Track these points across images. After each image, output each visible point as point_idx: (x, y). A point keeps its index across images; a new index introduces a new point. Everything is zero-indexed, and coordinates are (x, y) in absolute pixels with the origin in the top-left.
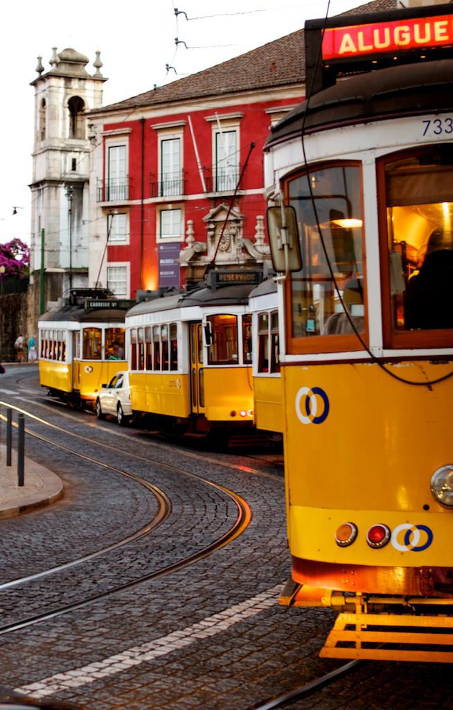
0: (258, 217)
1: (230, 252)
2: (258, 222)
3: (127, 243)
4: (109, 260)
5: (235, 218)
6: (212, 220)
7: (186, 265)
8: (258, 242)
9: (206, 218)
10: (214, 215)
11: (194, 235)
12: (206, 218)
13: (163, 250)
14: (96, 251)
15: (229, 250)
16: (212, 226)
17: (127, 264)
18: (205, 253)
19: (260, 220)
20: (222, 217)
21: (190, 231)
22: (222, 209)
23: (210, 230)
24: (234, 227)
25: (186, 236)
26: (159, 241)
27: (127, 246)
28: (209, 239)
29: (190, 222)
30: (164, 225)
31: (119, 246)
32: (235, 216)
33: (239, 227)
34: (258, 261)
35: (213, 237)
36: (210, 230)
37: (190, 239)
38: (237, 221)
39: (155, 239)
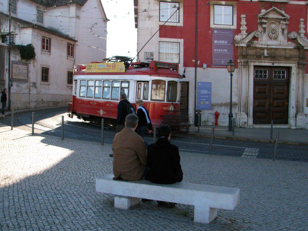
1: (278, 40)
2: (302, 22)
3: (181, 24)
4: (161, 36)
5: (285, 18)
8: (302, 35)
9: (260, 15)
10: (266, 14)
11: (246, 25)
12: (260, 15)
13: (217, 33)
14: (147, 28)
15: (278, 39)
17: (182, 41)
19: (302, 21)
20: (272, 16)
21: (243, 22)
22: (274, 10)
24: (283, 24)
25: (239, 25)
26: (212, 26)
27: (181, 27)
28: (260, 29)
29: (243, 16)
30: (216, 15)
31: (172, 26)
32: (283, 16)
33: (286, 24)
34: (305, 48)
35: (264, 29)
37: (244, 28)
38: (285, 20)
39: (209, 25)
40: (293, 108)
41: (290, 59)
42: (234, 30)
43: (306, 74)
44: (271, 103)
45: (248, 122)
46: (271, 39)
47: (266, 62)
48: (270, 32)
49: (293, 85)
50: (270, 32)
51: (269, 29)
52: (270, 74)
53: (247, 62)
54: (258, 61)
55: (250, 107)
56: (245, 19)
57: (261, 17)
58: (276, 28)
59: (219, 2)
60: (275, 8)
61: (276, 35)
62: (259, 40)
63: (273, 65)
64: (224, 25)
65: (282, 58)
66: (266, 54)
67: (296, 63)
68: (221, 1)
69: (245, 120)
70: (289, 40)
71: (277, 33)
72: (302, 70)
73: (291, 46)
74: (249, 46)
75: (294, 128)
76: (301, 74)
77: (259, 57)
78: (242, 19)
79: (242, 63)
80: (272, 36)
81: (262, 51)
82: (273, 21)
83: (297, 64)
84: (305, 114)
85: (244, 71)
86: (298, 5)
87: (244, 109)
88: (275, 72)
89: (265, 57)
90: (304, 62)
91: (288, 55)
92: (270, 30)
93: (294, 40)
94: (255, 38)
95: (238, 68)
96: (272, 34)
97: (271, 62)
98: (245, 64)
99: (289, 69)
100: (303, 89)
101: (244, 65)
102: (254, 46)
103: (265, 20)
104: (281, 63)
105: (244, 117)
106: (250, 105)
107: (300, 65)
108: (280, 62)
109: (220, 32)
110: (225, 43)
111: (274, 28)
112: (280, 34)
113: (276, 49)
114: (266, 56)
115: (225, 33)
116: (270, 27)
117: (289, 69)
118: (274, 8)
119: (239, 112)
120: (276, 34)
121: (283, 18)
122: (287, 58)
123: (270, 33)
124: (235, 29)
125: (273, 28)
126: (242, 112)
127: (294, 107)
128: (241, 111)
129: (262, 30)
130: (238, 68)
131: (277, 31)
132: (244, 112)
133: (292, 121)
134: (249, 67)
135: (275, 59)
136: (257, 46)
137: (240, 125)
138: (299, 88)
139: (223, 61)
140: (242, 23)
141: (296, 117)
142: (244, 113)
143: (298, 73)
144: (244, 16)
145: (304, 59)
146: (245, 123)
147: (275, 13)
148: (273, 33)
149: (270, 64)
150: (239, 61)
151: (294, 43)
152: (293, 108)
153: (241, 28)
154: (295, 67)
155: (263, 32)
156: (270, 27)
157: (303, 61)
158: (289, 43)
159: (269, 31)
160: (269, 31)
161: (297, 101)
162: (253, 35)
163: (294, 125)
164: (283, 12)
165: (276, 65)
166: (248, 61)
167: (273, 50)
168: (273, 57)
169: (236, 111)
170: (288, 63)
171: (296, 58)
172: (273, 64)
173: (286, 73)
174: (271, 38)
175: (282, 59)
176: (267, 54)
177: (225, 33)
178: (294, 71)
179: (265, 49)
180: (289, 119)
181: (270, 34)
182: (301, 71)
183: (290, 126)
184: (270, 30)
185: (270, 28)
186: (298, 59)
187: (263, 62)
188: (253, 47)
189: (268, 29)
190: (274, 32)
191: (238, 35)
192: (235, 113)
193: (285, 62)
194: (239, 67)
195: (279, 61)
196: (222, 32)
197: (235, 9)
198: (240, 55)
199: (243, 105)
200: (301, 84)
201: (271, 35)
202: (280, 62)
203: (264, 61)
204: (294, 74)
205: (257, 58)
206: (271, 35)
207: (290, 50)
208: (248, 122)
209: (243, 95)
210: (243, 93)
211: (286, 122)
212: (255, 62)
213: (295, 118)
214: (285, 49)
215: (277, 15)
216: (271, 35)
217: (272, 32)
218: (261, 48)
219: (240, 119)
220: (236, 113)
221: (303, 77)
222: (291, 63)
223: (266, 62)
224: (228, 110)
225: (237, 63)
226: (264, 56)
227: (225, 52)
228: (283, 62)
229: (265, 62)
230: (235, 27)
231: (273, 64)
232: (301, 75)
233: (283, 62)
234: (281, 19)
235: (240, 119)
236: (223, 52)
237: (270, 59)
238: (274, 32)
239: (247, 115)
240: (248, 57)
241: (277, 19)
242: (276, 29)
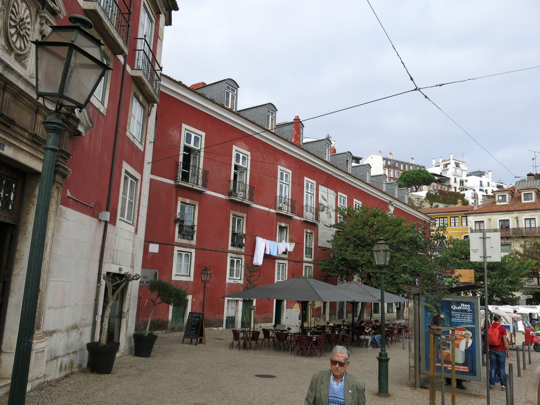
34: (80, 129)
43: (61, 206)
50: (13, 24)
51: (12, 12)
65: (26, 134)
96: (15, 36)
116: (14, 6)
123: (11, 27)
135: (8, 131)
148: (19, 34)
175: (24, 137)
181: (13, 31)
193: (31, 152)
206: (14, 38)
216: (12, 36)
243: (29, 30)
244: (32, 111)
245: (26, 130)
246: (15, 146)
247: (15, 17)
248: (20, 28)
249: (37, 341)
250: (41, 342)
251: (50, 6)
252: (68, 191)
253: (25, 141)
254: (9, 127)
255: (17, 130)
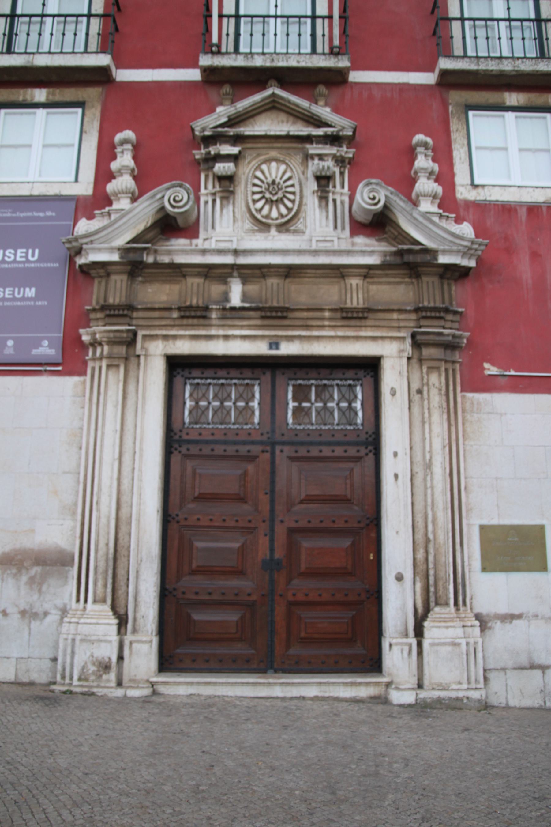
0: (419, 137)
2: (420, 149)
5: (329, 130)
6: (231, 132)
7: (115, 257)
8: (426, 206)
10: (234, 121)
15: (300, 225)
16: (227, 149)
18: (190, 230)
19: (425, 145)
23: (219, 158)
24: (321, 157)
25: (104, 175)
34: (443, 259)
36: (219, 158)
40: (399, 578)
41: (369, 323)
42: (77, 200)
43: (469, 395)
44: (277, 556)
45: (121, 658)
46: (260, 231)
47: (235, 337)
48: (257, 197)
49: (395, 454)
50: (257, 197)
51: (255, 185)
52: (273, 405)
53: (131, 342)
54: (188, 333)
55: (137, 577)
56: (129, 147)
57: (207, 133)
58: (290, 178)
59: (22, 91)
60: (279, 92)
61: (289, 210)
62: (202, 234)
63: (274, 352)
64: (33, 183)
65: (327, 314)
66: (236, 300)
67: (403, 338)
68: (29, 91)
69: (109, 652)
70: (358, 227)
71: (293, 201)
72: (438, 368)
73: (369, 251)
74: (134, 265)
75: (408, 698)
76: (434, 392)
77: (194, 315)
78: (119, 150)
79: (100, 344)
80: (267, 217)
81: (216, 289)
82: (274, 154)
83: (409, 341)
84: (478, 617)
85: (114, 381)
86: (403, 87)
87: (105, 586)
88: (301, 394)
89: (231, 314)
90: (446, 331)
91: (356, 301)
92: (256, 189)
93: (379, 224)
94: (168, 225)
95: (83, 373)
96: (267, 207)
97: (263, 337)
98: (122, 350)
99: (371, 366)
100: (453, 474)
101: (109, 357)
102: (166, 259)
103: (234, 145)
104: (318, 338)
105: (100, 630)
106: (139, 562)
107: (428, 345)
108: (316, 333)
109: (9, 215)
110: (28, 261)
111: (278, 180)
112: (312, 202)
113: (290, 272)
114: (233, 309)
115: (35, 214)
116: (256, 177)
117: (371, 366)
118: (273, 94)
119: (78, 600)
120: (290, 205)
121: (320, 132)
122: (352, 317)
123: (255, 201)
124: (85, 198)
125: (270, 180)
126: (95, 601)
127: (408, 575)
128: (86, 601)
129: (218, 188)
130: (84, 373)
131: (294, 193)
132: (104, 601)
133: (396, 657)
134: (139, 364)
136: (180, 259)
137: (71, 678)
138: (429, 466)
139: (10, 343)
140: (114, 166)
141: (419, 632)
142: (106, 608)
143: (420, 392)
144: (129, 134)
145: (450, 317)
146: (106, 667)
147: (283, 116)
148: (270, 202)
149: (260, 348)
150: (86, 338)
151: (386, 240)
152: (399, 578)
153: (111, 187)
154: (401, 357)
155: (222, 198)
156: (258, 174)
157: (444, 328)
158: (361, 241)
159: (254, 193)
160: (254, 193)
161: (422, 543)
162: (156, 206)
163: (414, 681)
164: (323, 111)
165: (288, 349)
166: (135, 334)
167: (273, 281)
168: (272, 309)
169: (66, 601)
170: (357, 338)
171: (400, 311)
172: (274, 345)
173: (360, 396)
174: (263, 226)
175: (323, 319)
176: (245, 297)
177: (35, 214)
178: (393, 376)
179: (231, 276)
180: (383, 639)
181: (259, 205)
182: (434, 378)
183: (388, 685)
184: (256, 189)
185: (257, 182)
186: (413, 316)
187: (217, 337)
188: (156, 265)
189: (246, 187)
190: (280, 195)
191: (91, 217)
192: (56, 607)
193: (340, 333)
194: (90, 364)
195: (307, 327)
196: (18, 214)
197: (94, 114)
198: (94, 310)
199: (102, 564)
200: (438, 444)
201: (265, 211)
202: (316, 333)
203: (221, 332)
204: (393, 393)
205: (185, 322)
206: (265, 211)
207: (367, 272)
208: (121, 658)
209: (104, 508)
210: (104, 499)
211: (373, 664)
212: (175, 337)
213: (414, 642)
214: (339, 272)
215: (294, 123)
217: (268, 195)
218: (209, 272)
219: (74, 640)
220: (65, 605)
221: (452, 413)
222: (374, 338)
223: (235, 337)
224: (19, 589)
225: (83, 347)
226: (224, 309)
227: (23, 299)
228: (332, 333)
229: (226, 337)
230: (85, 188)
231: (274, 345)
232: (436, 399)
233: (332, 333)
234: (308, 139)
235: (74, 640)
236: (14, 299)
237: (258, 322)
238: (280, 195)
239: (122, 622)
240: (135, 315)
241: (288, 138)
242: (289, 183)
243: (293, 186)
244: (336, 280)
245: (321, 310)
246: (300, 337)
247: (261, 187)
248: (271, 193)
249: (432, 624)
250: (447, 627)
251: (319, 136)
252: (486, 365)
253: (327, 323)
254: (285, 318)
255: (305, 314)
